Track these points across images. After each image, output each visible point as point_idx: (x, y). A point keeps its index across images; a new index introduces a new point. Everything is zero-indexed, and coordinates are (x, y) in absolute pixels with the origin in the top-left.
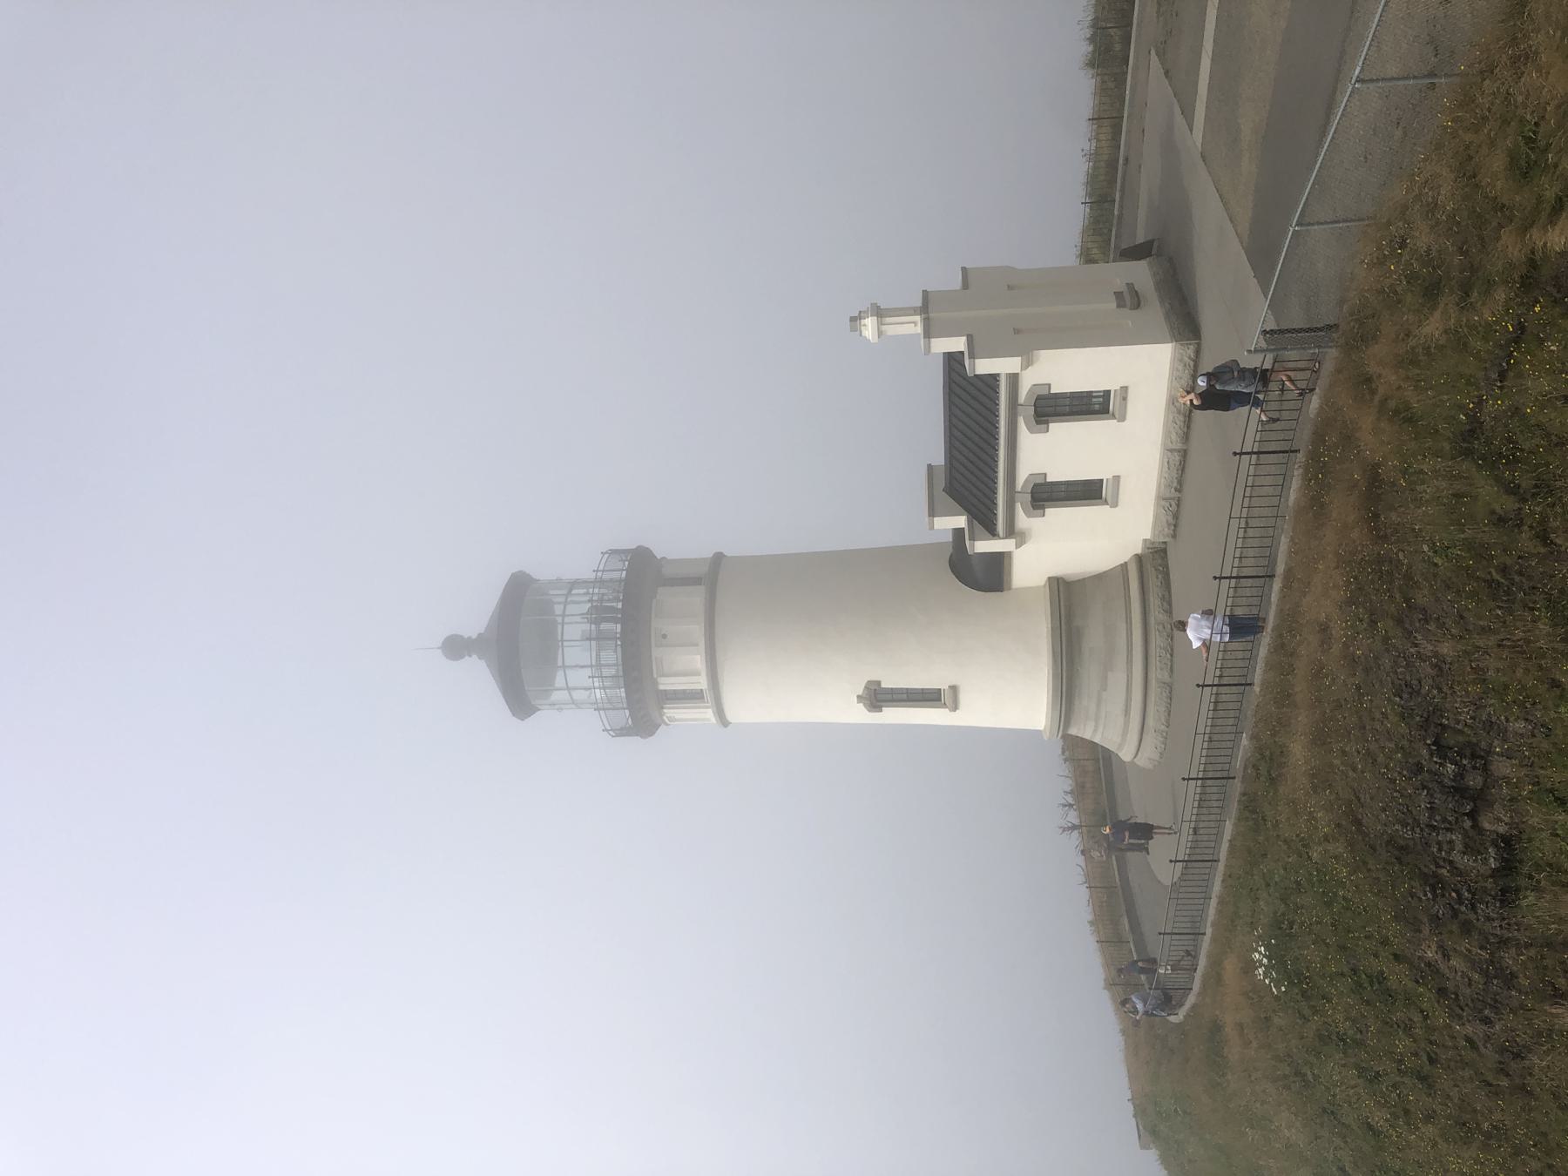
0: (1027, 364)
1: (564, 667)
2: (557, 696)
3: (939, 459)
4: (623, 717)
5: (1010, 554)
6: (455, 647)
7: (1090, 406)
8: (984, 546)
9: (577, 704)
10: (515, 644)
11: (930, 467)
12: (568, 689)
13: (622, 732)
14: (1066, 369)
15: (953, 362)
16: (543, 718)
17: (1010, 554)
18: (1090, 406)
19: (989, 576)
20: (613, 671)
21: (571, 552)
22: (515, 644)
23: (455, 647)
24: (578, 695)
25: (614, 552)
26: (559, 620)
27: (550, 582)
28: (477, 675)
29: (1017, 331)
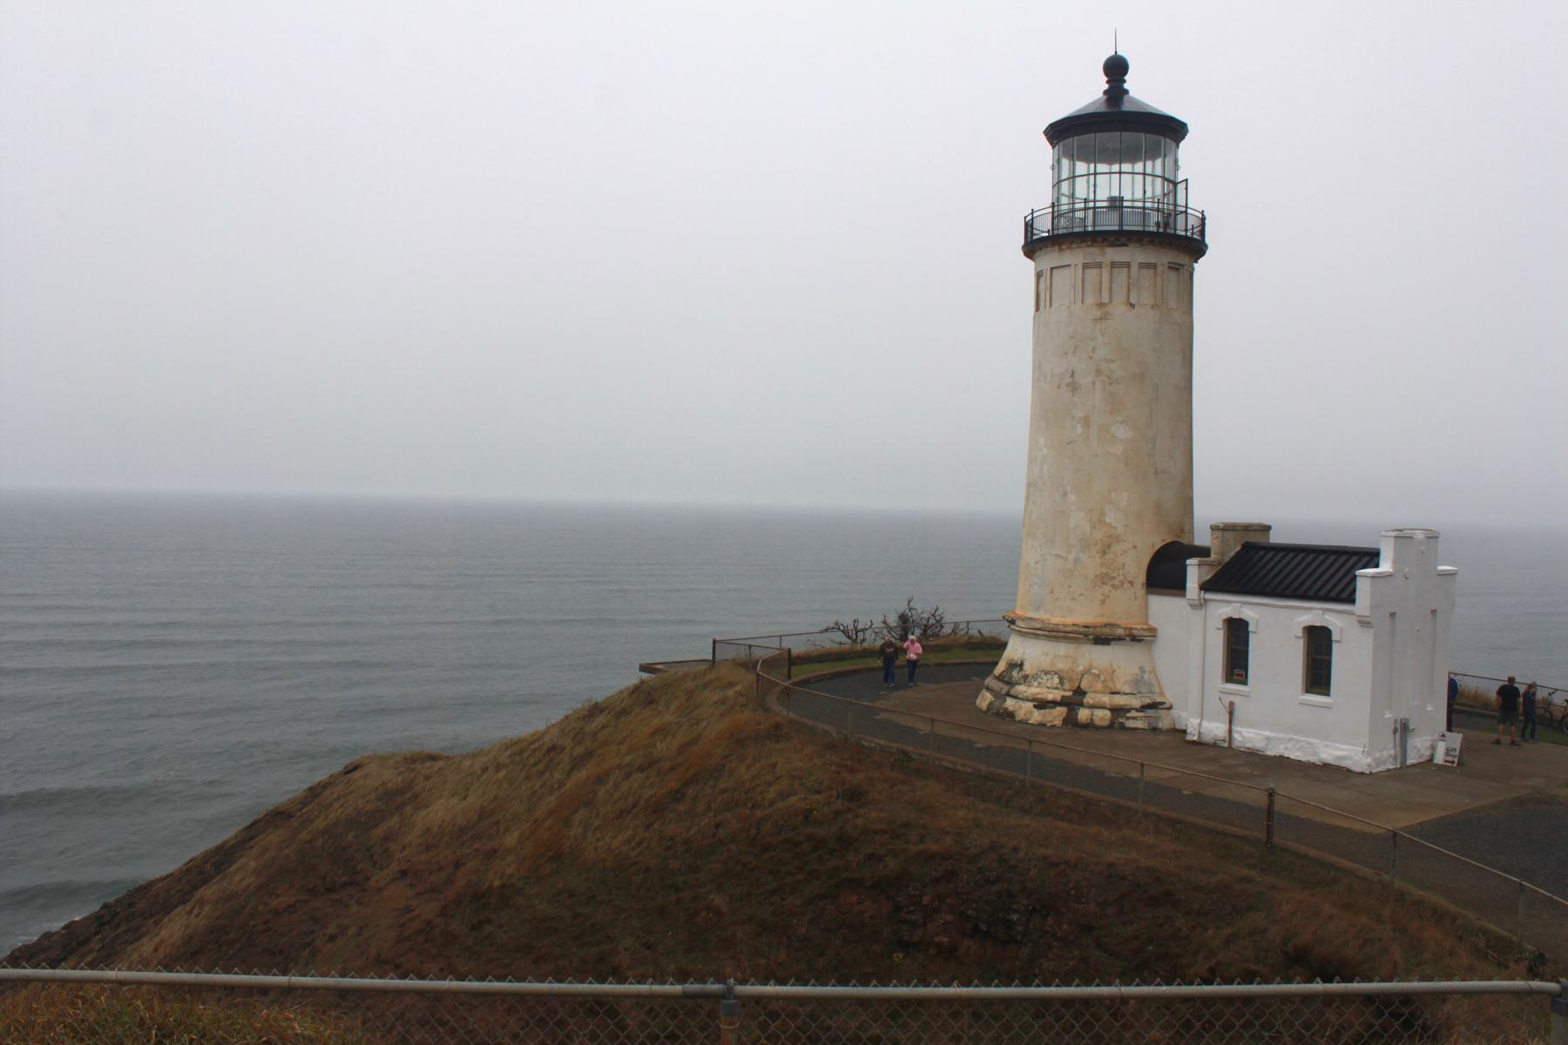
0: (1364, 623)
1: (1095, 174)
2: (1065, 162)
3: (1275, 538)
4: (1044, 227)
5: (1184, 595)
6: (1116, 69)
7: (1318, 676)
8: (1194, 573)
9: (1057, 184)
10: (1117, 125)
11: (1267, 529)
12: (1073, 177)
13: (1029, 227)
14: (1352, 657)
15: (1370, 557)
16: (1046, 151)
17: (1184, 595)
18: (1318, 676)
19: (1165, 572)
20: (1090, 221)
21: (1206, 176)
22: (1117, 125)
23: (1116, 69)
24: (1065, 187)
25: (1203, 219)
26: (1139, 167)
27: (1176, 161)
28: (1089, 92)
29: (1393, 615)
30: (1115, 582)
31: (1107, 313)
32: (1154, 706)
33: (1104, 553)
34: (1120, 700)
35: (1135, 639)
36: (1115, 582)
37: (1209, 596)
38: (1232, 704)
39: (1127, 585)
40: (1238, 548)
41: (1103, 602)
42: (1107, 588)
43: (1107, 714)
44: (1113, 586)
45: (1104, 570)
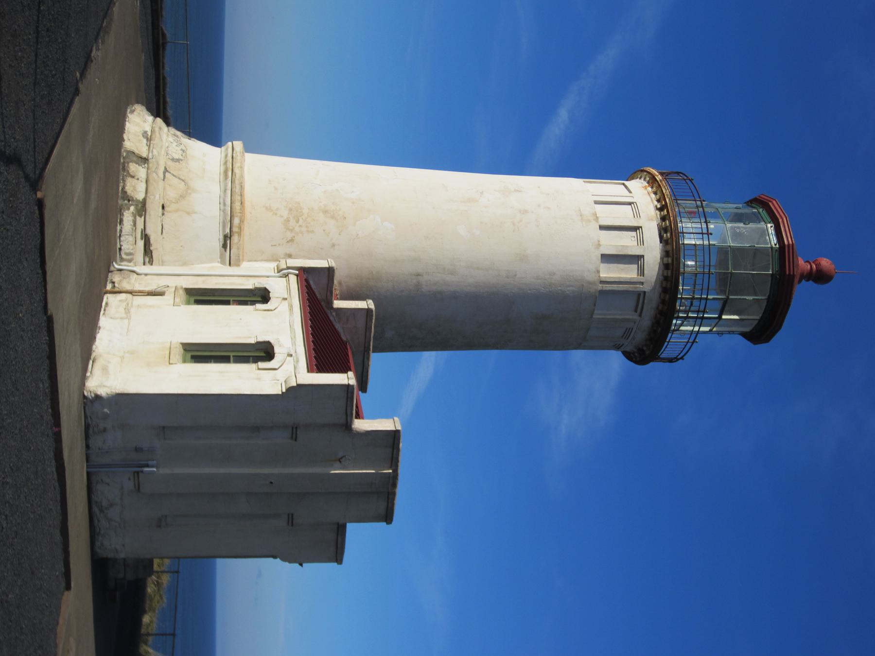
30: (292, 223)
31: (589, 221)
32: (148, 251)
33: (325, 212)
34: (153, 209)
35: (227, 241)
36: (292, 223)
37: (293, 279)
38: (161, 294)
39: (289, 235)
40: (344, 338)
41: (268, 209)
42: (285, 213)
43: (140, 196)
44: (288, 220)
45: (305, 211)
